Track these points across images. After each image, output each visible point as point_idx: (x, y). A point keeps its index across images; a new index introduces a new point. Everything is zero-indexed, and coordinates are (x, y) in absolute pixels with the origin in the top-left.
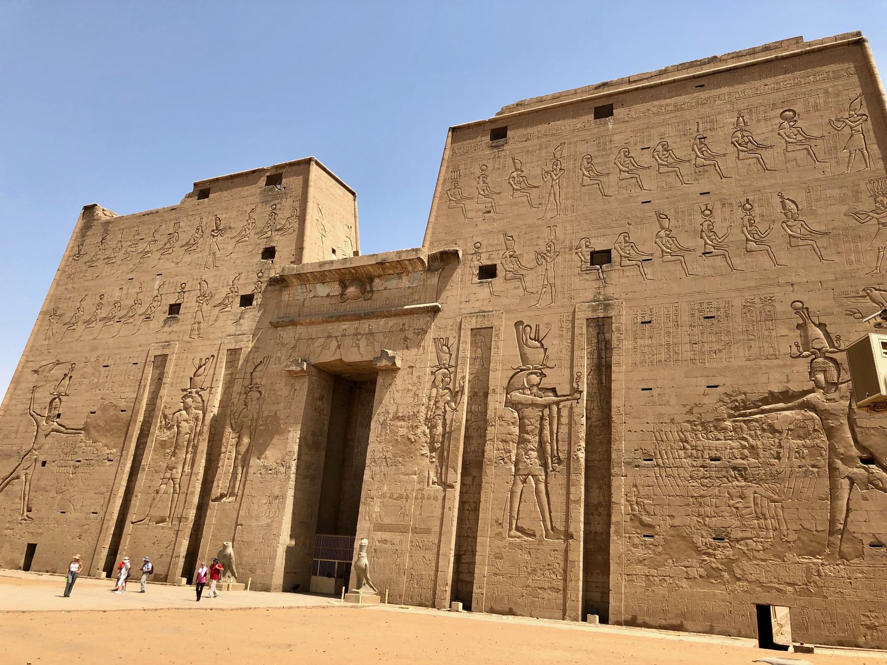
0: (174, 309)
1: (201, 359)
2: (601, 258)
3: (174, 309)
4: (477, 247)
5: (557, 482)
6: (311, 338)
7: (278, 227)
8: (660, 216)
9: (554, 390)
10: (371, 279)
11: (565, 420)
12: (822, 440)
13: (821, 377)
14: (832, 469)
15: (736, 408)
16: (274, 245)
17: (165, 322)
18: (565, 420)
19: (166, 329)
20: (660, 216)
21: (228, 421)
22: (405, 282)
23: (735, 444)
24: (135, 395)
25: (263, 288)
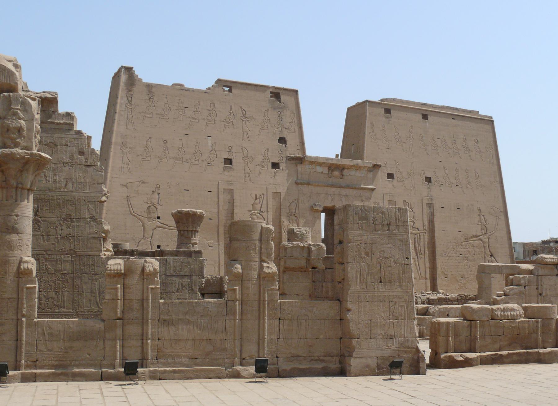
0: (229, 162)
1: (256, 195)
2: (428, 180)
3: (229, 162)
4: (386, 163)
5: (421, 261)
6: (317, 193)
7: (285, 126)
8: (444, 167)
9: (418, 228)
10: (344, 169)
11: (422, 240)
12: (483, 250)
13: (483, 231)
14: (485, 258)
15: (465, 239)
16: (285, 136)
17: (225, 169)
18: (422, 240)
19: (226, 173)
20: (444, 167)
21: (283, 230)
22: (358, 174)
23: (465, 250)
24: (216, 210)
25: (284, 161)
